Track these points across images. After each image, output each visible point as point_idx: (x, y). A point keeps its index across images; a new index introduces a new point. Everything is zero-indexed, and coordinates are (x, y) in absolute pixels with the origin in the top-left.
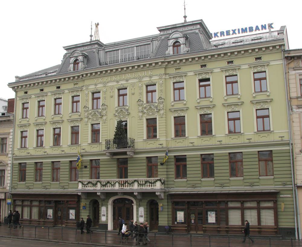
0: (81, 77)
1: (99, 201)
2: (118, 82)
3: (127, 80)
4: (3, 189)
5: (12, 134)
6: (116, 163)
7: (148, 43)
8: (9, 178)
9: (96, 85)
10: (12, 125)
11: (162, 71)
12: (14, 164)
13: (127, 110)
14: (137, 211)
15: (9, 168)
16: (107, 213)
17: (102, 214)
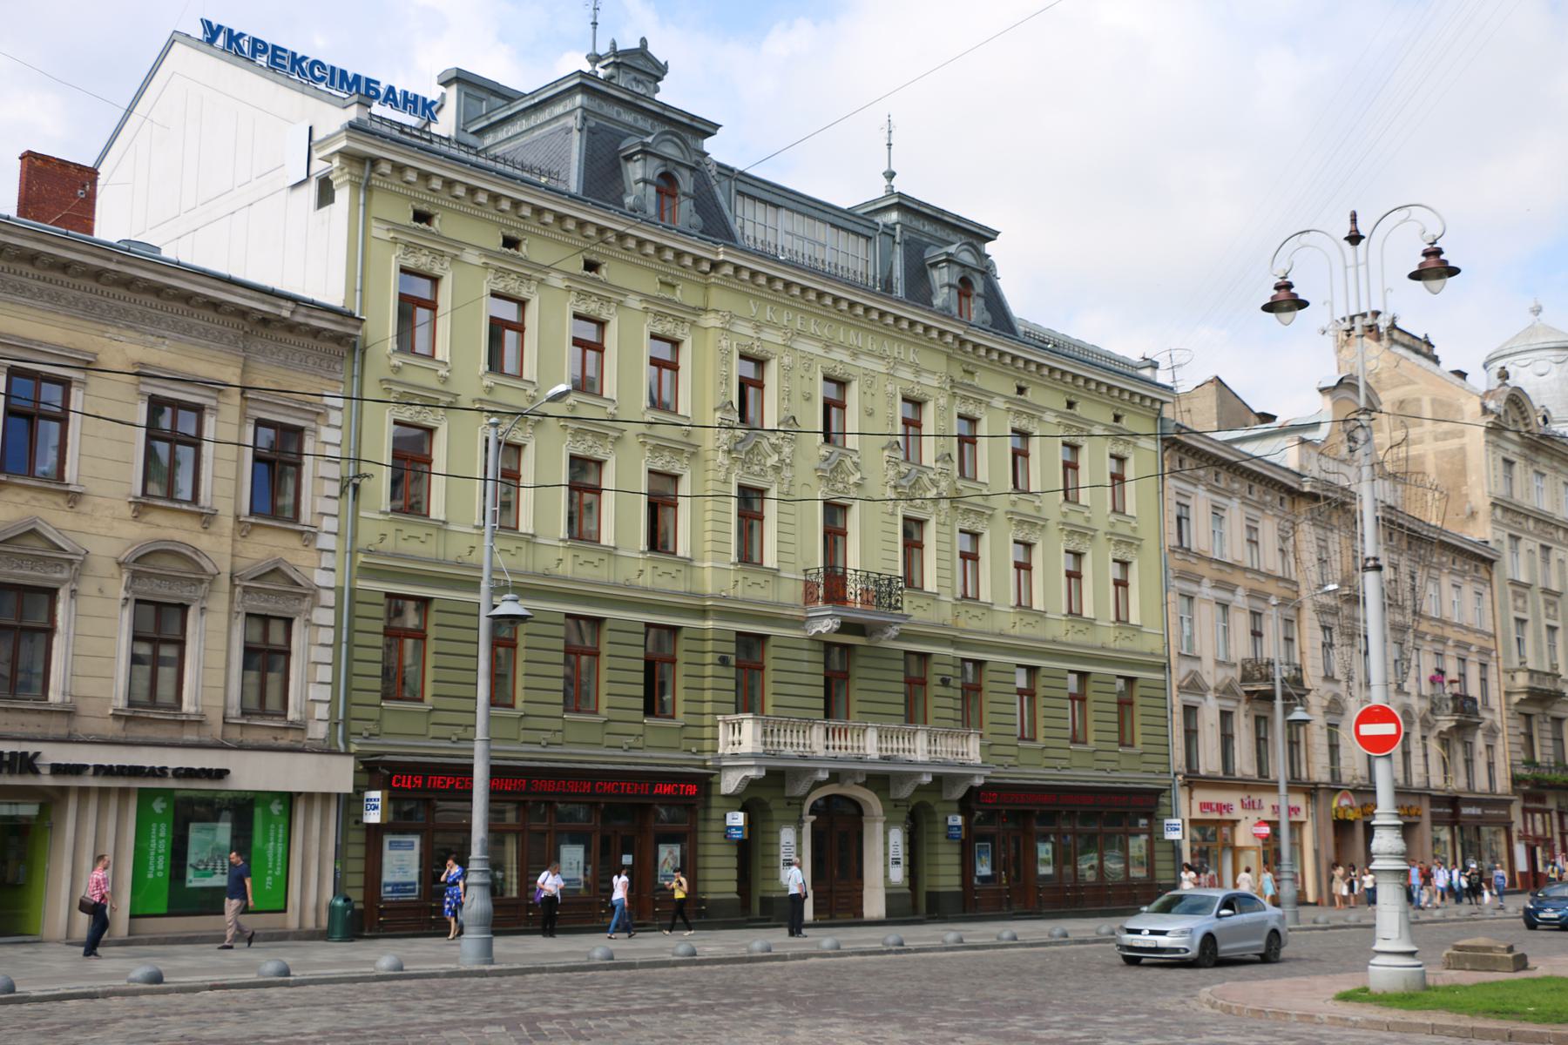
0: (706, 267)
1: (772, 805)
2: (828, 346)
3: (855, 355)
4: (279, 734)
5: (336, 418)
6: (821, 657)
7: (870, 233)
8: (325, 674)
9: (758, 327)
10: (338, 367)
11: (938, 363)
12: (359, 597)
13: (856, 465)
14: (886, 843)
15: (327, 617)
16: (799, 855)
17: (783, 856)
